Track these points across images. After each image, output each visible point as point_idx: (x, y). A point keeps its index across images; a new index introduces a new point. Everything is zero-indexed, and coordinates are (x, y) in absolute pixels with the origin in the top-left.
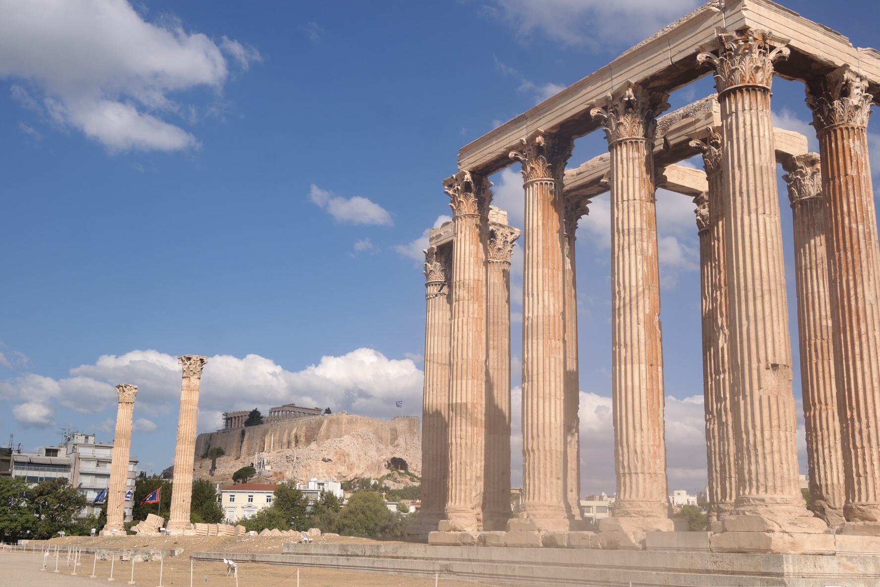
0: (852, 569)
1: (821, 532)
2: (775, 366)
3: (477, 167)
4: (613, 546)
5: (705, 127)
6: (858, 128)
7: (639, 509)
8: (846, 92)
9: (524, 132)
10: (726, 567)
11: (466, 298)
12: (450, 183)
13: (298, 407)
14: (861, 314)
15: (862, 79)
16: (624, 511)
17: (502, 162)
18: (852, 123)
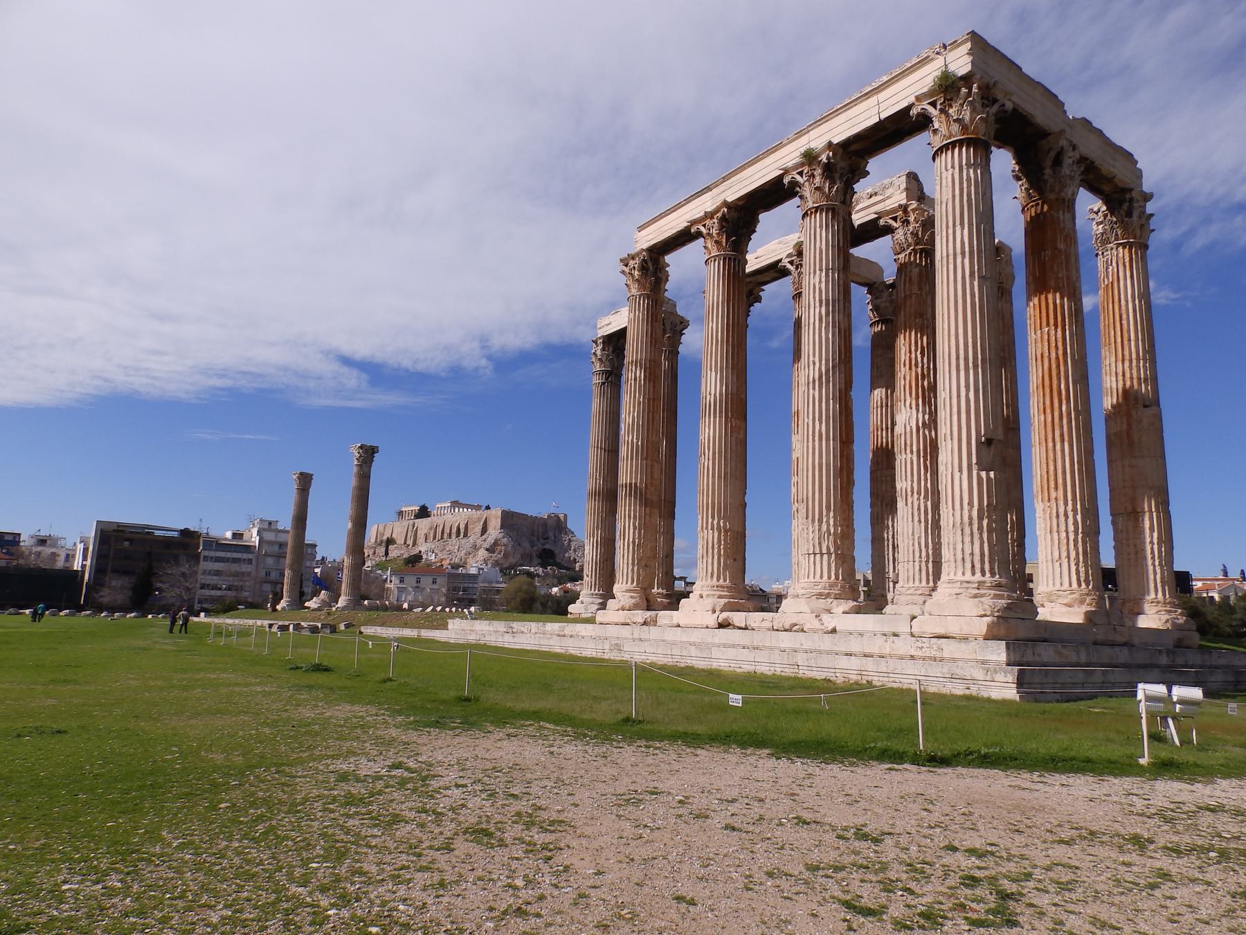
7: (827, 591)
8: (1058, 162)
9: (709, 204)
10: (933, 653)
15: (1074, 148)
17: (684, 238)
18: (1063, 194)
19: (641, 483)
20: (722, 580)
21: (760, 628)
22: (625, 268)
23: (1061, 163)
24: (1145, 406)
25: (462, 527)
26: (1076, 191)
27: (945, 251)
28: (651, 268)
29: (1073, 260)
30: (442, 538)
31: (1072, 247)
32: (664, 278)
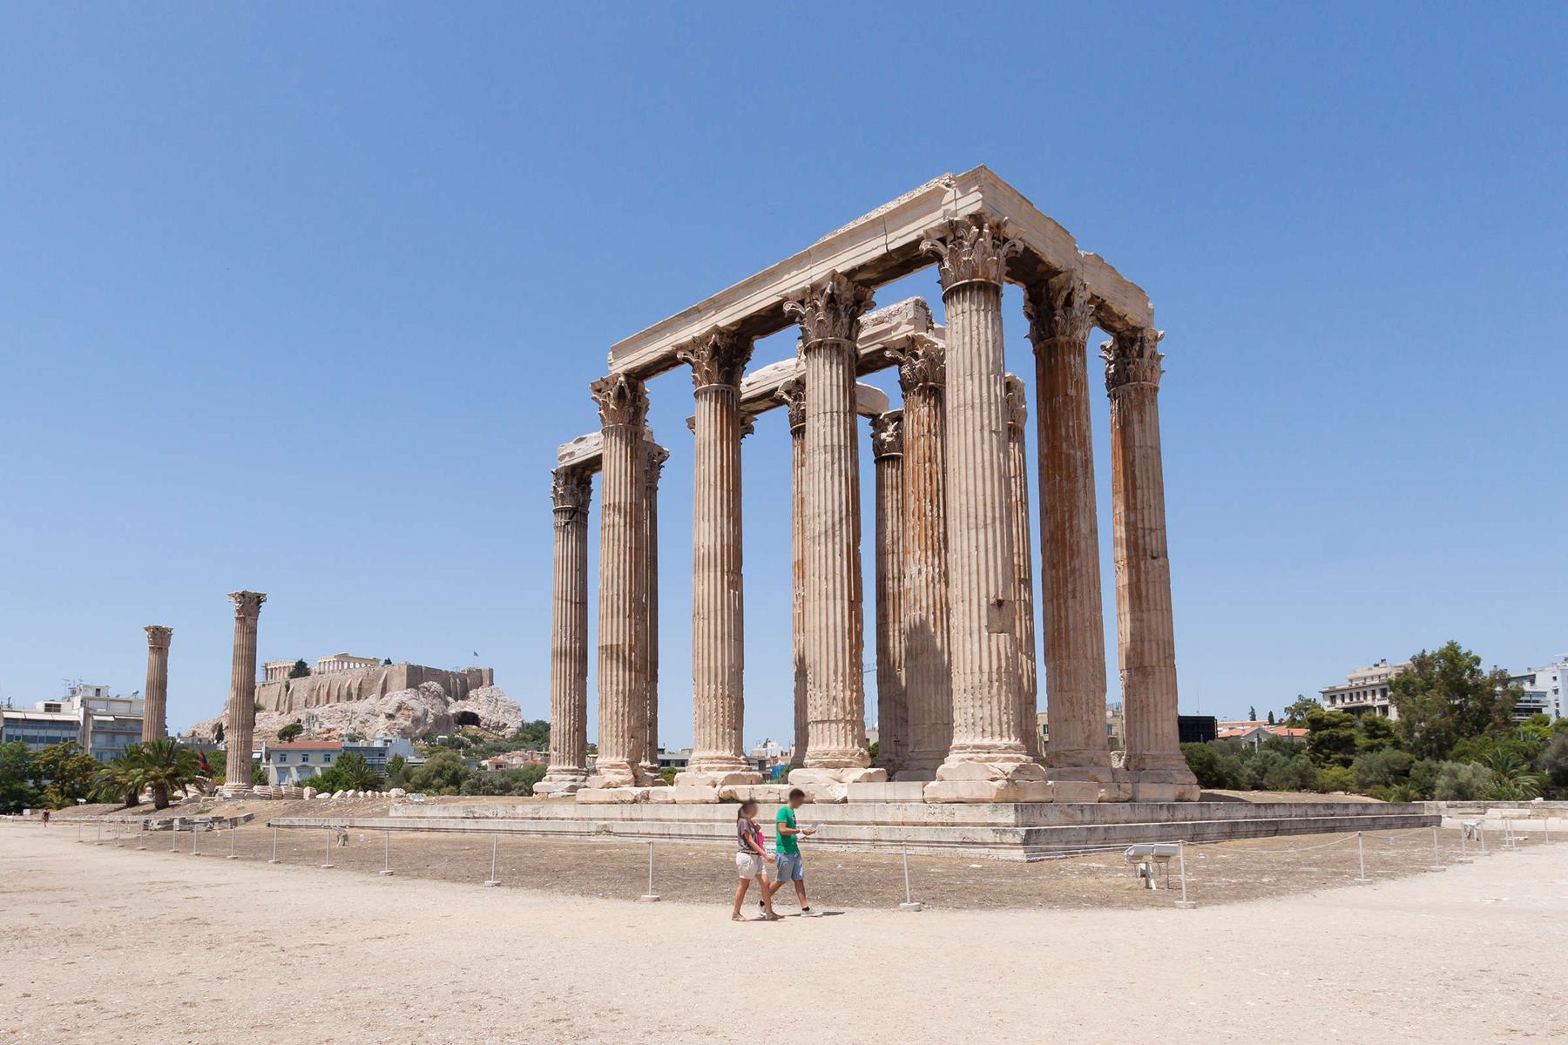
5: (905, 335)
10: (945, 819)
13: (352, 657)
14: (1075, 548)
16: (820, 762)
24: (1153, 558)
25: (355, 686)
27: (956, 402)
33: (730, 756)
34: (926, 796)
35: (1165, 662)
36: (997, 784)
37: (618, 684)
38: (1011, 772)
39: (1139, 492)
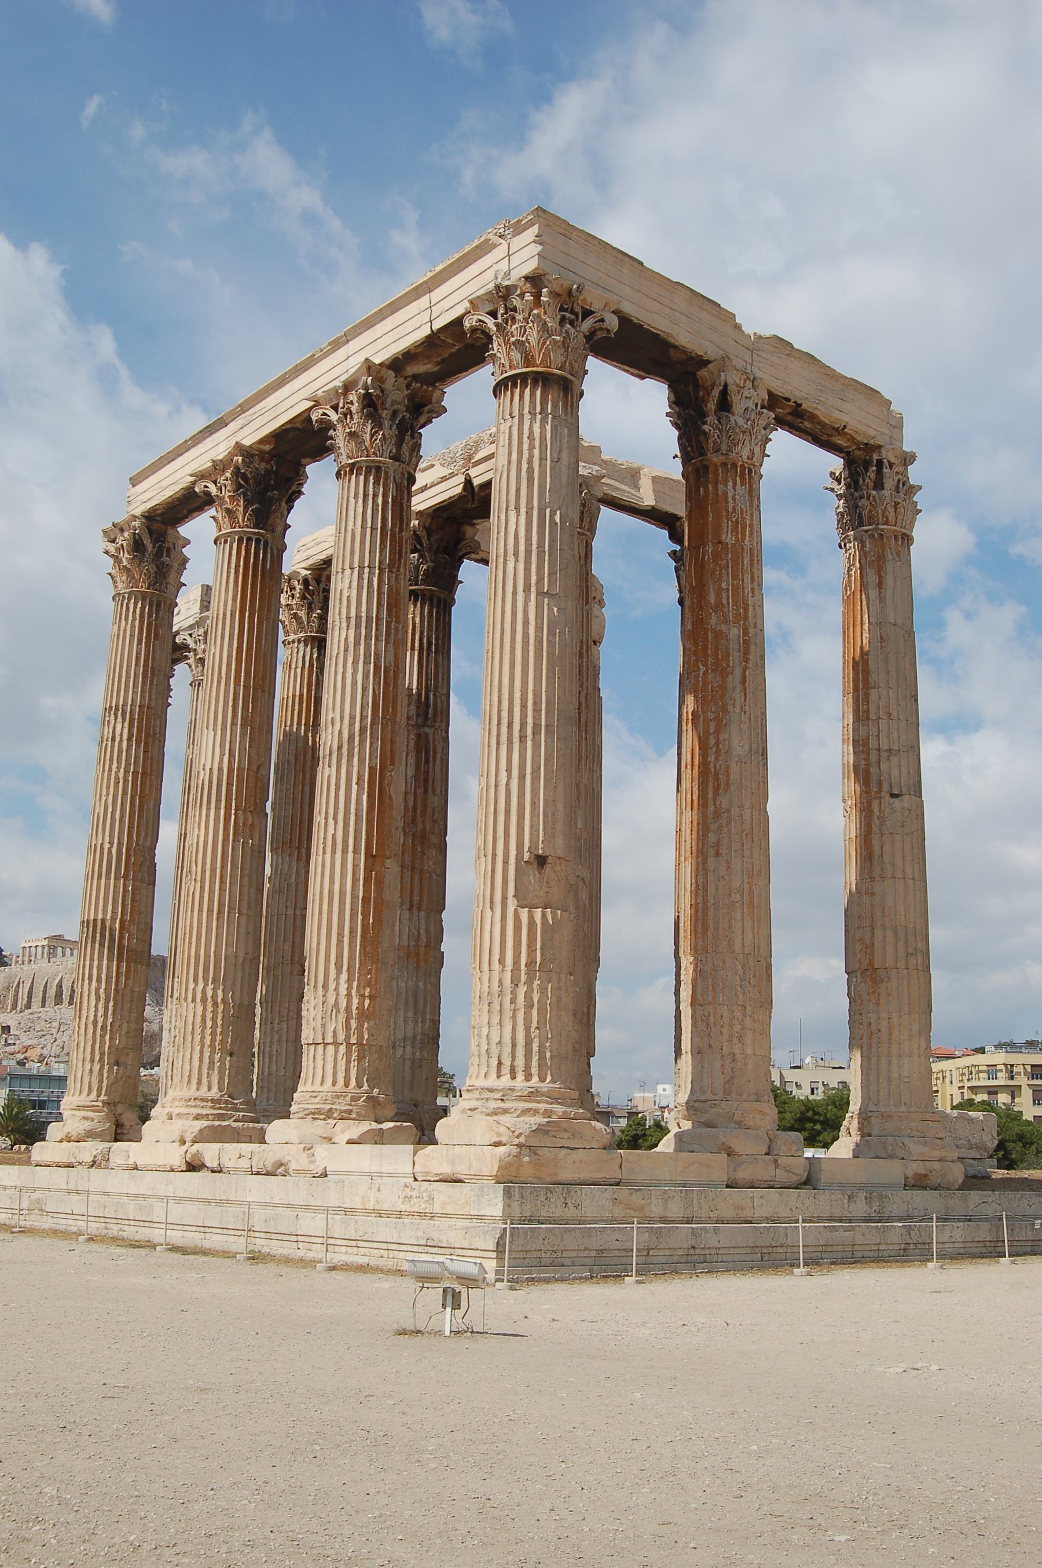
0: (641, 1209)
1: (600, 1145)
2: (541, 861)
3: (153, 509)
4: (277, 1170)
6: (742, 466)
7: (328, 1107)
8: (725, 405)
11: (125, 736)
12: (113, 537)
13: (69, 941)
19: (113, 919)
20: (204, 1088)
21: (236, 1169)
22: (111, 547)
23: (731, 406)
24: (893, 795)
26: (757, 449)
28: (149, 547)
29: (746, 561)
30: (28, 1006)
31: (747, 542)
32: (176, 565)
33: (217, 1096)
34: (418, 1168)
35: (907, 963)
36: (501, 1150)
37: (99, 980)
38: (528, 1133)
39: (873, 693)
